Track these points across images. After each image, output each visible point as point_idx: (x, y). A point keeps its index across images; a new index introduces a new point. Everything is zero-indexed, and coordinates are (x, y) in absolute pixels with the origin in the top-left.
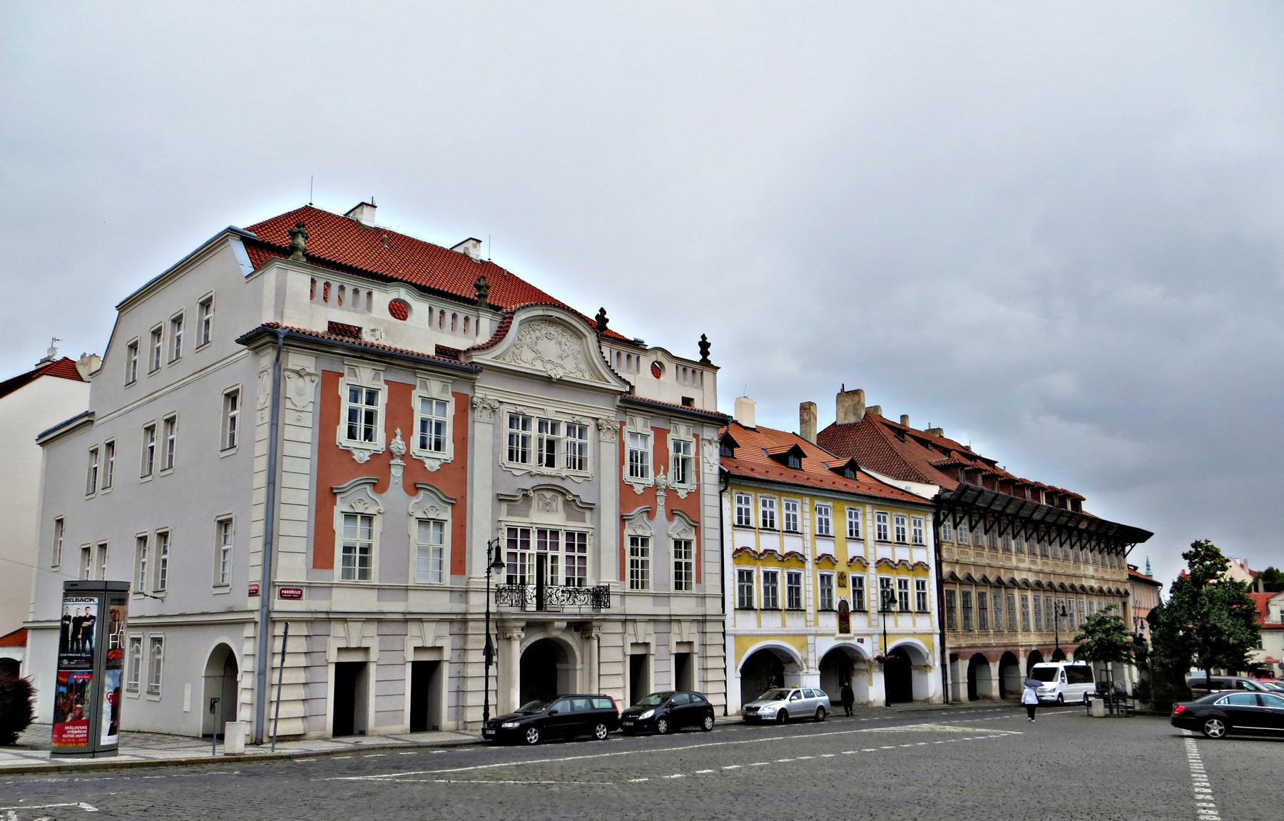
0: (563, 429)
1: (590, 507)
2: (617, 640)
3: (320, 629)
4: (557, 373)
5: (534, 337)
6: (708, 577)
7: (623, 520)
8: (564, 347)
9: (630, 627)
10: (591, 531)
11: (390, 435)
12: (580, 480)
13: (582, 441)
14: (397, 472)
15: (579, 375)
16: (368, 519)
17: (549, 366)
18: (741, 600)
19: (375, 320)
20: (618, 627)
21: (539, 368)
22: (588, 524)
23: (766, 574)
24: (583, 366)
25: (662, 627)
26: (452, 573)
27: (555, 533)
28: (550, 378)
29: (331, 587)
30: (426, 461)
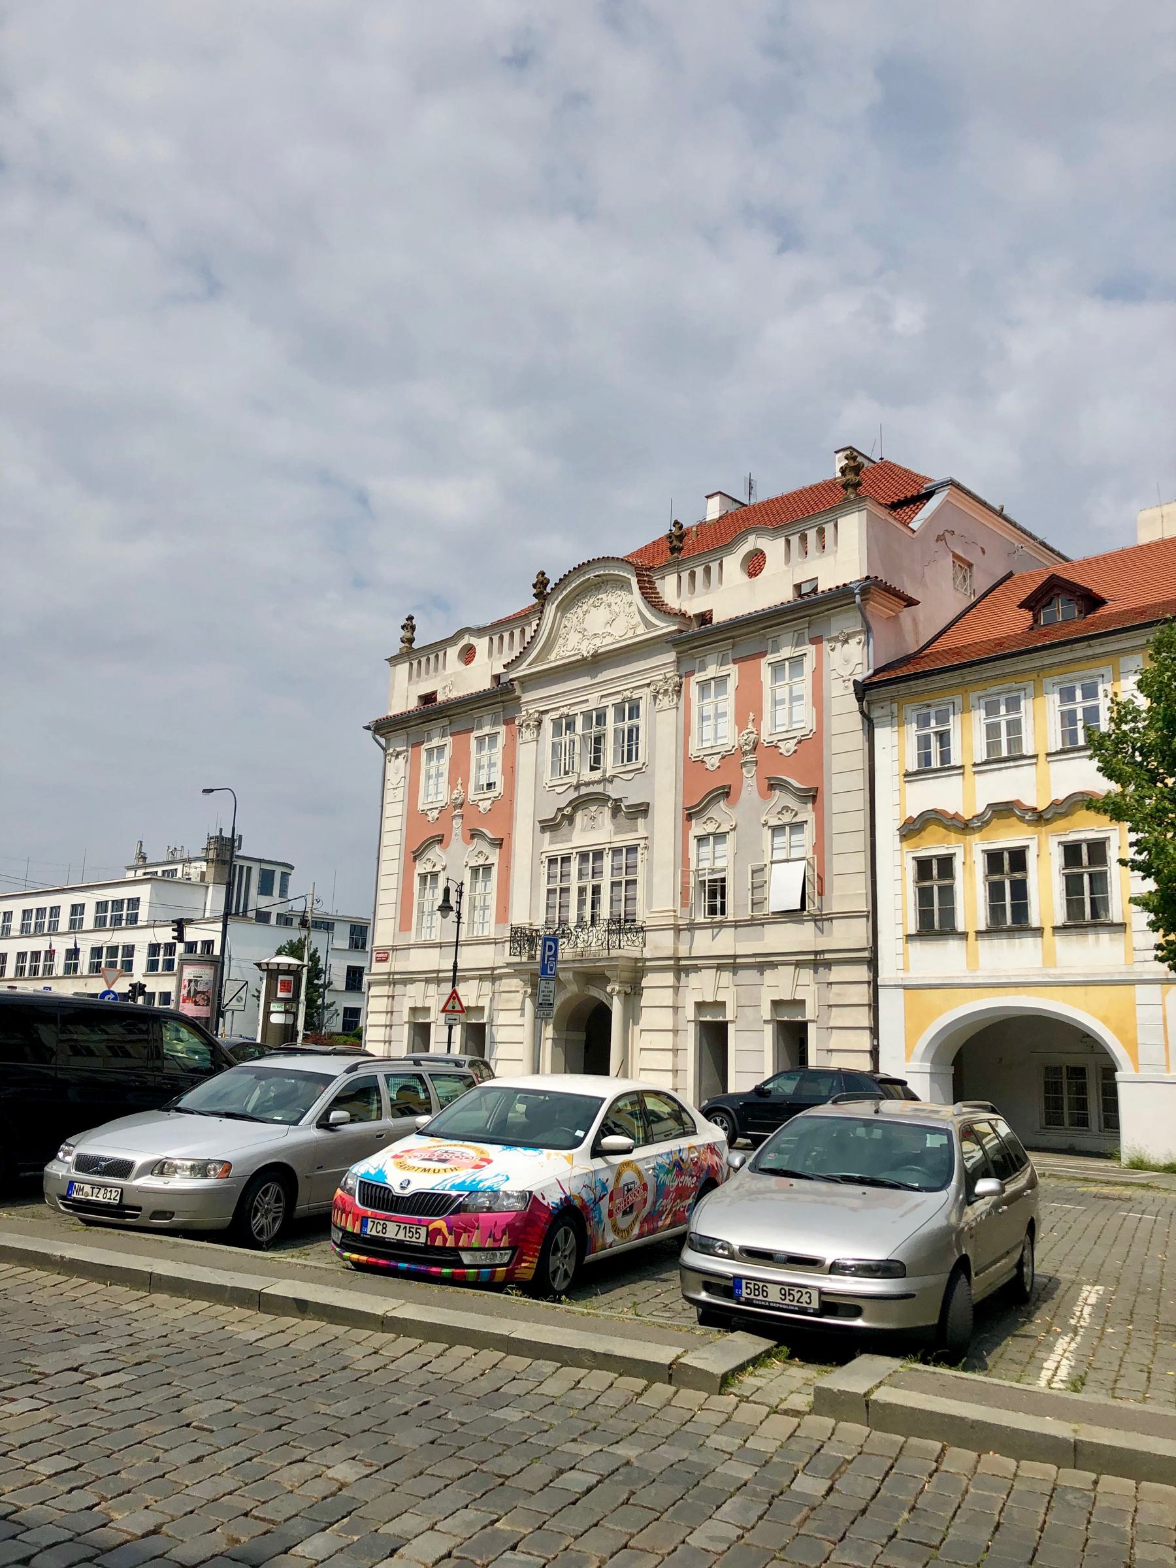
0: (611, 714)
1: (642, 810)
2: (667, 997)
3: (399, 989)
4: (605, 644)
5: (581, 615)
6: (837, 882)
7: (689, 817)
8: (613, 606)
9: (694, 979)
10: (642, 842)
11: (452, 783)
12: (631, 776)
13: (634, 722)
14: (456, 823)
15: (630, 634)
16: (435, 875)
18: (925, 916)
20: (668, 978)
21: (586, 649)
22: (642, 833)
23: (994, 859)
24: (638, 618)
25: (746, 976)
26: (497, 922)
27: (598, 855)
28: (584, 659)
29: (409, 947)
30: (480, 803)
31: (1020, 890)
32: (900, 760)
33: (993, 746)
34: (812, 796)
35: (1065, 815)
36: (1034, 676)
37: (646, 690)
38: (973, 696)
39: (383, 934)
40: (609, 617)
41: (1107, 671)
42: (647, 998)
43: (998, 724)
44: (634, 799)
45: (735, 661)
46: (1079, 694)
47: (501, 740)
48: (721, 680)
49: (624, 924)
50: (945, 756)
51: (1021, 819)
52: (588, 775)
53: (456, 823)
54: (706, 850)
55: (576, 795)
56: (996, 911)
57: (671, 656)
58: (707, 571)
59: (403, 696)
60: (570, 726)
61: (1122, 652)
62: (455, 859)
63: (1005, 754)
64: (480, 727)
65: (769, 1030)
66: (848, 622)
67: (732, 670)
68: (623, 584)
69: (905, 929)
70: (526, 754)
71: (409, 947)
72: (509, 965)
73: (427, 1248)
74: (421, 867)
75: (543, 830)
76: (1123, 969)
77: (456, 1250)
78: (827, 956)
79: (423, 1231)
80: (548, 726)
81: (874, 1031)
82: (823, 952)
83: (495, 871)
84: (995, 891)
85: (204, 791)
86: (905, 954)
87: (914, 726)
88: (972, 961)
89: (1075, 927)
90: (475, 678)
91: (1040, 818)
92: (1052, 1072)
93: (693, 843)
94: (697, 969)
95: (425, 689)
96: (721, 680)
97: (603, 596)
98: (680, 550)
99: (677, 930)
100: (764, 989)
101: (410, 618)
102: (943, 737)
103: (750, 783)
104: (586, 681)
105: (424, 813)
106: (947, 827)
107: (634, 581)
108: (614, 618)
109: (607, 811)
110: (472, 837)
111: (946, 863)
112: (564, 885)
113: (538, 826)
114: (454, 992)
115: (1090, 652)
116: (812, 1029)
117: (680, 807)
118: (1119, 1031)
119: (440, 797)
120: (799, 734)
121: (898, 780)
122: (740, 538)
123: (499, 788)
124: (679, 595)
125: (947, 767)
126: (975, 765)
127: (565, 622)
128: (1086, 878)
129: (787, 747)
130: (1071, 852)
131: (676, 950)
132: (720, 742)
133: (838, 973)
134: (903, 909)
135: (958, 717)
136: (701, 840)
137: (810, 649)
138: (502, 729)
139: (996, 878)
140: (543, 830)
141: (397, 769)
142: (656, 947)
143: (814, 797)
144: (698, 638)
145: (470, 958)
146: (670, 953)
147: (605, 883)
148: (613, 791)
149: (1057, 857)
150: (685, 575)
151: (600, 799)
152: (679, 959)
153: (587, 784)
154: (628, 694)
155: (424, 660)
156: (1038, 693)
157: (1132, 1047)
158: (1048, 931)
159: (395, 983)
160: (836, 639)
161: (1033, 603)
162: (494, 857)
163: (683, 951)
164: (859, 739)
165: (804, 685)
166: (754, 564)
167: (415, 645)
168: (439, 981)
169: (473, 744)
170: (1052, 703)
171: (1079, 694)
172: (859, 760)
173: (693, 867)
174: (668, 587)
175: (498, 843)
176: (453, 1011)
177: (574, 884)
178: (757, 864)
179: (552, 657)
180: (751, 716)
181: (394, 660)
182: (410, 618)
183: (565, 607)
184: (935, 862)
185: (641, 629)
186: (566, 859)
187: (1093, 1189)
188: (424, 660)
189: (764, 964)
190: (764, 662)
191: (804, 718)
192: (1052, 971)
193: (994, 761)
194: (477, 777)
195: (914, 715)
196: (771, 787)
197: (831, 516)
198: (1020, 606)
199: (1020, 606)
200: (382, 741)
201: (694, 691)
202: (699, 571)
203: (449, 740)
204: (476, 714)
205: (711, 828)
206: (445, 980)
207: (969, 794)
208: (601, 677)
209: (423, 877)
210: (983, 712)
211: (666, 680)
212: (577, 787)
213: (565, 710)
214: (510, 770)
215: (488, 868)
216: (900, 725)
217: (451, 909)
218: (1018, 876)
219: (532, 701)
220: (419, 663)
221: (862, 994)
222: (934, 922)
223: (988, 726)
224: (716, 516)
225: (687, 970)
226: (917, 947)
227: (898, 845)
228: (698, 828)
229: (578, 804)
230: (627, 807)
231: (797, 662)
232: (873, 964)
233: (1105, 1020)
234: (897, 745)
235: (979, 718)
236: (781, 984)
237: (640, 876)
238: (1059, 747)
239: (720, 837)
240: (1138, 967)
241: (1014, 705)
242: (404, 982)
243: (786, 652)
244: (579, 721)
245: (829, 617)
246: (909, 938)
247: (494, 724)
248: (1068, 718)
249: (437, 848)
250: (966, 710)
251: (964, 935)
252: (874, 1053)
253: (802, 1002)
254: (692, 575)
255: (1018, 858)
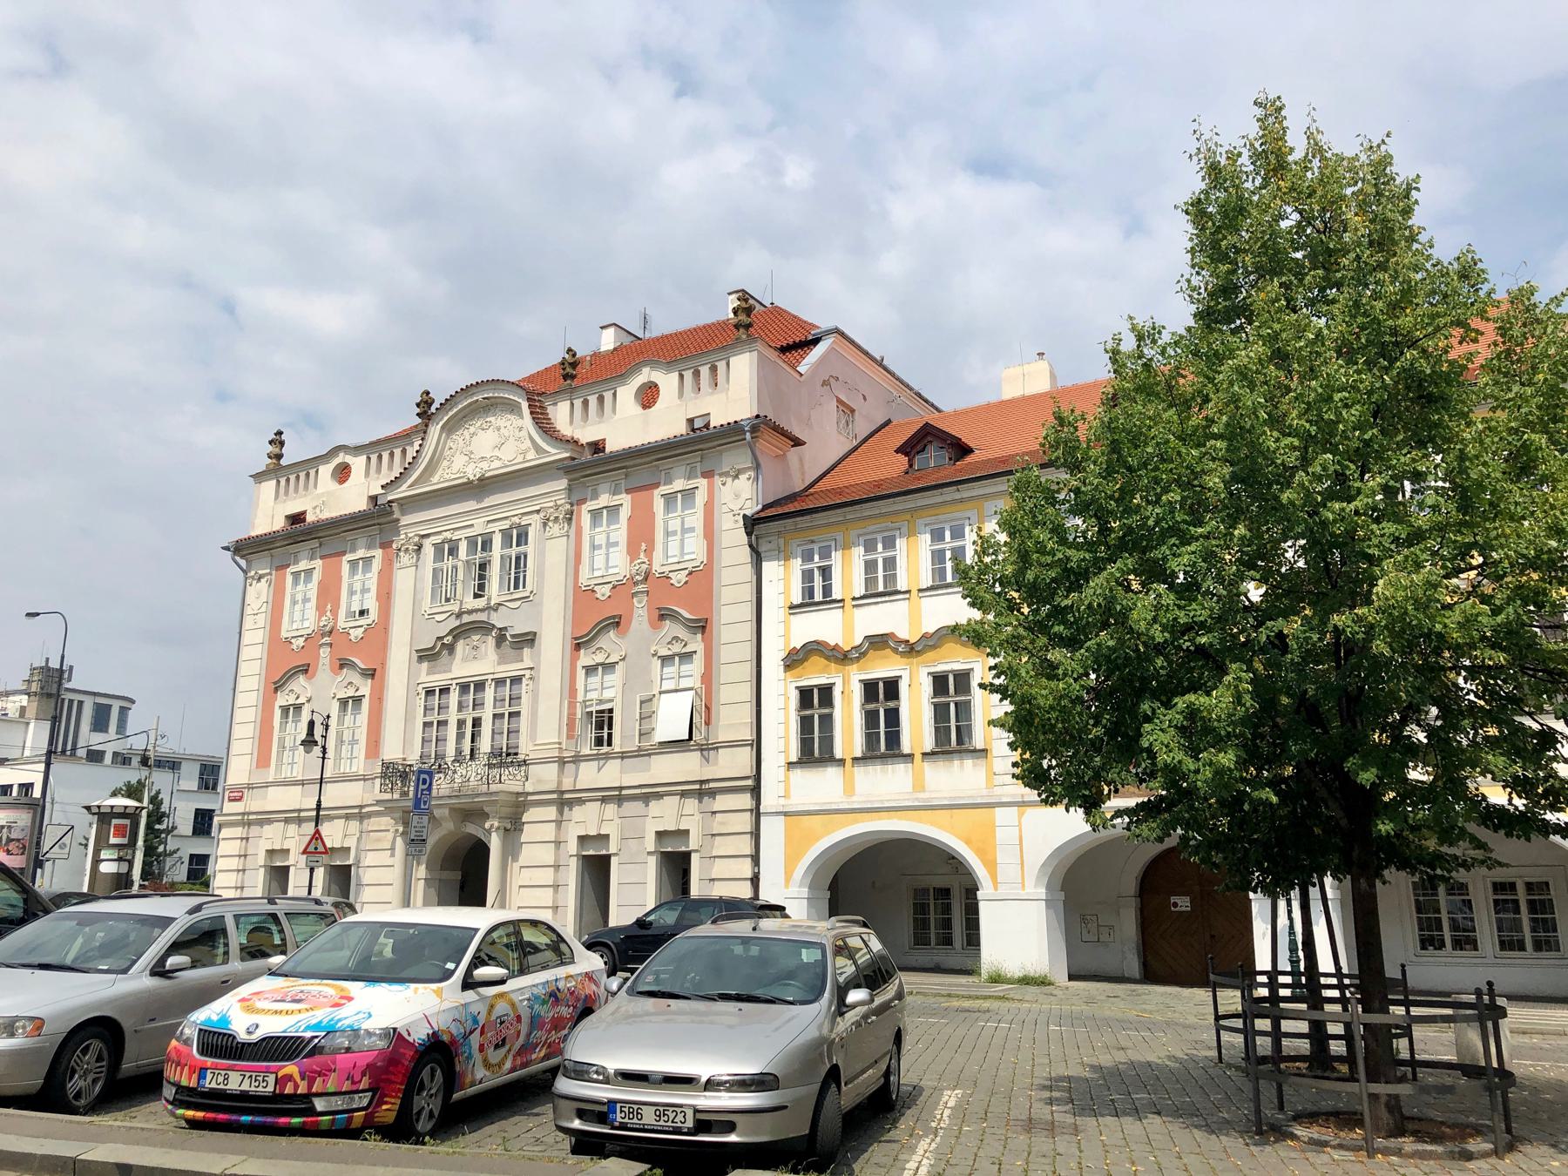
0: (497, 540)
2: (549, 832)
3: (255, 830)
4: (494, 468)
7: (578, 647)
9: (577, 813)
10: (528, 673)
11: (321, 610)
13: (522, 549)
14: (324, 652)
15: (520, 459)
16: (298, 708)
17: (485, 465)
19: (319, 496)
20: (551, 812)
21: (473, 472)
22: (527, 663)
23: (870, 688)
24: (528, 443)
25: (631, 808)
26: (367, 757)
27: (480, 686)
29: (267, 785)
31: (893, 717)
32: (786, 592)
33: (870, 581)
34: (701, 626)
35: (934, 647)
36: (908, 516)
37: (535, 516)
38: (853, 533)
39: (237, 772)
40: (498, 440)
41: (973, 514)
42: (528, 833)
43: (876, 561)
44: (519, 625)
45: (628, 491)
46: (948, 534)
47: (376, 565)
48: (613, 510)
49: (506, 757)
50: (827, 590)
51: (895, 651)
52: (471, 603)
53: (324, 652)
54: (595, 680)
55: (454, 623)
56: (871, 739)
57: (563, 483)
58: (601, 399)
59: (268, 513)
60: (453, 551)
61: (985, 497)
62: (321, 690)
63: (880, 589)
64: (353, 550)
65: (652, 862)
66: (742, 458)
67: (625, 500)
68: (514, 408)
69: (787, 756)
70: (404, 579)
71: (267, 785)
72: (379, 802)
73: (275, 1098)
74: (283, 699)
75: (421, 659)
76: (985, 792)
77: (308, 1097)
78: (712, 785)
79: (271, 1079)
80: (428, 550)
81: (756, 859)
82: (708, 781)
83: (365, 703)
84: (871, 719)
85: (28, 615)
86: (787, 781)
87: (799, 560)
88: (849, 789)
89: (943, 753)
90: (352, 498)
91: (911, 650)
92: (921, 893)
93: (581, 673)
94: (581, 802)
95: (294, 508)
96: (613, 510)
97: (492, 419)
98: (573, 377)
99: (562, 762)
100: (648, 820)
101: (280, 433)
102: (826, 572)
103: (640, 612)
104: (471, 505)
105: (288, 641)
106: (828, 658)
107: (525, 405)
108: (502, 442)
109: (491, 641)
110: (342, 666)
111: (826, 692)
112: (442, 718)
113: (415, 656)
114: (317, 832)
115: (958, 496)
116: (695, 858)
117: (569, 637)
118: (981, 853)
119: (306, 624)
120: (690, 565)
121: (783, 613)
122: (636, 369)
123: (373, 615)
124: (571, 422)
125: (828, 600)
126: (854, 599)
127: (450, 443)
128: (952, 706)
129: (679, 578)
130: (940, 682)
131: (560, 783)
132: (611, 571)
133: (722, 802)
134: (786, 737)
135: (839, 553)
136: (590, 670)
137: (702, 483)
138: (378, 553)
139: (871, 706)
140: (421, 659)
141: (259, 593)
142: (539, 781)
143: (704, 627)
144: (590, 467)
145: (335, 796)
146: (553, 787)
147: (487, 715)
148: (498, 620)
149: (927, 686)
150: (578, 403)
151: (484, 628)
152: (563, 792)
153: (470, 612)
154: (516, 520)
155: (292, 478)
156: (911, 533)
157: (992, 866)
158: (918, 757)
159: (249, 824)
160: (726, 474)
161: (911, 448)
162: (365, 688)
163: (567, 784)
164: (748, 572)
165: (696, 519)
166: (648, 396)
167: (283, 462)
168: (300, 821)
169: (346, 568)
170: (924, 541)
171: (948, 534)
172: (748, 592)
173: (580, 698)
174: (561, 414)
175: (370, 674)
176: (316, 852)
177: (453, 717)
178: (646, 694)
179: (435, 479)
180: (644, 547)
181: (259, 477)
182: (280, 433)
183: (449, 429)
184: (816, 691)
185: (532, 455)
186: (445, 691)
187: (956, 1003)
188: (292, 478)
189: (649, 795)
190: (657, 493)
191: (695, 550)
192: (922, 795)
193: (871, 595)
194: (349, 602)
195: (799, 550)
196: (662, 617)
197: (723, 354)
198: (897, 451)
199: (897, 451)
200: (243, 563)
201: (586, 519)
202: (593, 400)
203: (318, 563)
204: (350, 536)
205: (600, 658)
206: (308, 819)
207: (848, 627)
208: (488, 502)
209: (285, 710)
210: (862, 549)
211: (557, 507)
212: (459, 615)
213: (448, 535)
214: (385, 596)
215: (358, 700)
216: (787, 559)
217: (316, 743)
218: (891, 704)
219: (411, 524)
220: (288, 480)
221: (744, 822)
222: (815, 750)
223: (866, 562)
224: (611, 347)
225: (571, 803)
226: (798, 775)
227: (782, 674)
228: (586, 658)
229: (460, 633)
230: (513, 636)
231: (689, 494)
232: (756, 791)
233: (968, 842)
234: (783, 578)
235: (858, 554)
236: (665, 814)
237: (524, 707)
238: (930, 583)
239: (609, 667)
240: (998, 791)
241: (889, 544)
242: (261, 823)
243: (679, 484)
244: (463, 546)
245: (721, 453)
246: (790, 765)
247: (369, 548)
248: (938, 557)
249: (301, 678)
250: (846, 547)
251: (842, 762)
252: (755, 881)
253: (685, 833)
254: (586, 403)
255: (892, 687)
